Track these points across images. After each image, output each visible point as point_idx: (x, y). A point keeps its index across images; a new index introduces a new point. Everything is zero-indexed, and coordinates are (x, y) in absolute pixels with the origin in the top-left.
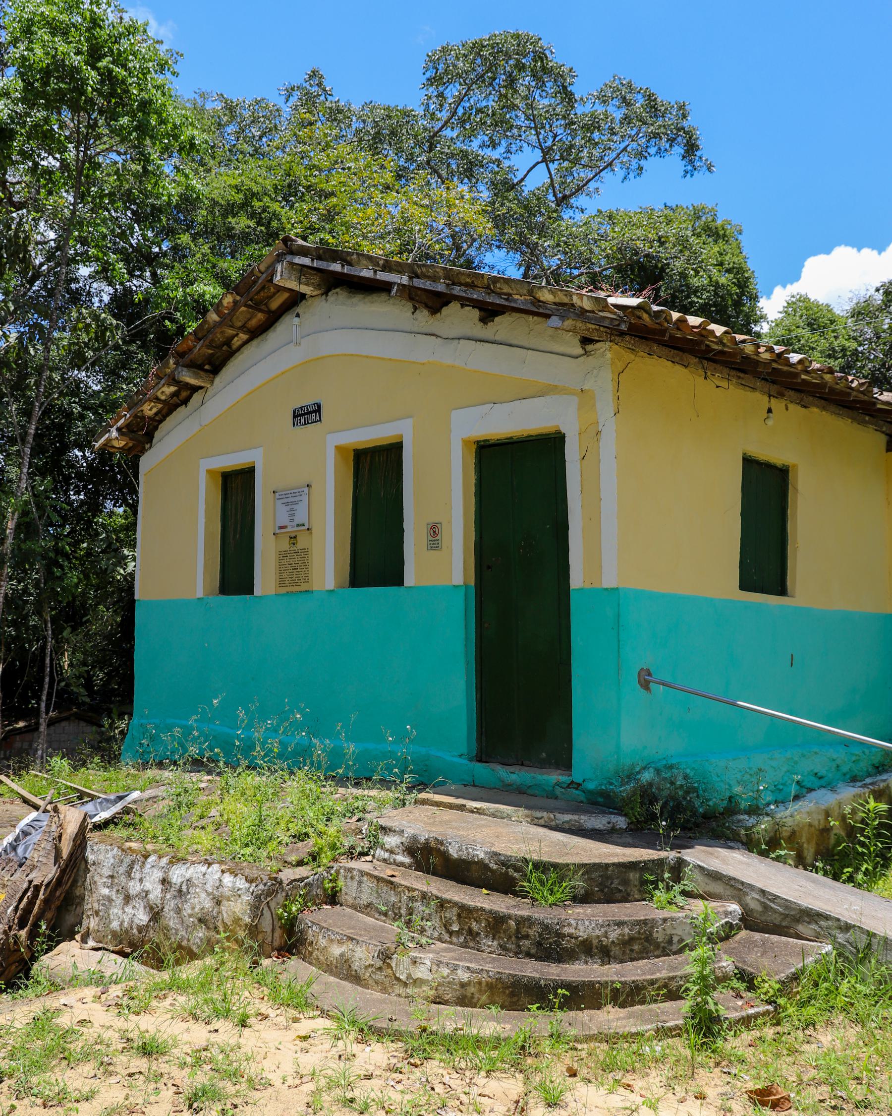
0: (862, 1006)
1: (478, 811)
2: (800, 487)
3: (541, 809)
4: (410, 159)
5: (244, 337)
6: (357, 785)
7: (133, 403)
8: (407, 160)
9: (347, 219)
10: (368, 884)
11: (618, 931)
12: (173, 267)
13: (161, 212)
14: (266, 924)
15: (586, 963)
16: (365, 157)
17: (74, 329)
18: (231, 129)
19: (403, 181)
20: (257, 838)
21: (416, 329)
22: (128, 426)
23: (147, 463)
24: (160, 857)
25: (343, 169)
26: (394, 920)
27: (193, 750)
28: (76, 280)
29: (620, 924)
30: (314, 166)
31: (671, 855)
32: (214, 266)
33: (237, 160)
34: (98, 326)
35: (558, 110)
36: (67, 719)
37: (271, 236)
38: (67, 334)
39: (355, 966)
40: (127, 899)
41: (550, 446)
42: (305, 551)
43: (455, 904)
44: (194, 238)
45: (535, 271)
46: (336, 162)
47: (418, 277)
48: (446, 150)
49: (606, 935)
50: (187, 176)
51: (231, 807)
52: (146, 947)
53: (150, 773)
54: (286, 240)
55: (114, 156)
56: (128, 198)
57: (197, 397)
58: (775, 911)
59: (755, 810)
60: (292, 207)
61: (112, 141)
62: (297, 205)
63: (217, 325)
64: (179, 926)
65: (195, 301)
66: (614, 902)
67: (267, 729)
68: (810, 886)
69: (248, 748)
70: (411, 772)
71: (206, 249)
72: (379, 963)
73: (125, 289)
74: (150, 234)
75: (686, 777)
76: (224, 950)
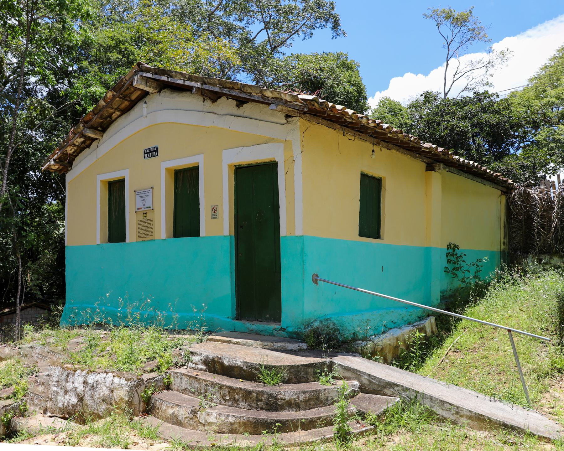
0: (413, 424)
1: (237, 343)
3: (267, 341)
4: (199, 26)
5: (118, 113)
6: (179, 333)
7: (61, 147)
8: (198, 26)
9: (168, 55)
10: (185, 379)
11: (304, 396)
12: (79, 78)
13: (73, 49)
14: (136, 400)
15: (289, 411)
16: (176, 24)
17: (28, 109)
18: (108, 7)
19: (196, 37)
20: (130, 360)
21: (205, 110)
22: (59, 158)
23: (69, 177)
24: (82, 371)
25: (166, 30)
26: (198, 395)
27: (97, 319)
28: (29, 84)
29: (304, 392)
30: (151, 28)
31: (328, 360)
32: (101, 78)
33: (111, 23)
34: (41, 108)
36: (30, 307)
37: (130, 63)
38: (25, 112)
39: (180, 418)
40: (66, 392)
41: (270, 168)
42: (151, 220)
43: (227, 387)
44: (90, 63)
45: (262, 83)
46: (162, 26)
47: (206, 84)
48: (217, 22)
49: (298, 398)
50: (85, 31)
51: (117, 346)
52: (77, 414)
53: (75, 331)
54: (139, 64)
55: (47, 19)
56: (55, 41)
57: (94, 144)
58: (375, 384)
59: (365, 339)
60: (140, 49)
61: (46, 12)
62: (142, 47)
63: (104, 107)
64: (92, 404)
65: (91, 95)
66: (302, 382)
67: (133, 307)
68: (390, 372)
69: (124, 317)
70: (204, 326)
71: (96, 69)
72: (191, 416)
73: (54, 89)
74: (67, 60)
75: (334, 324)
76: (115, 414)
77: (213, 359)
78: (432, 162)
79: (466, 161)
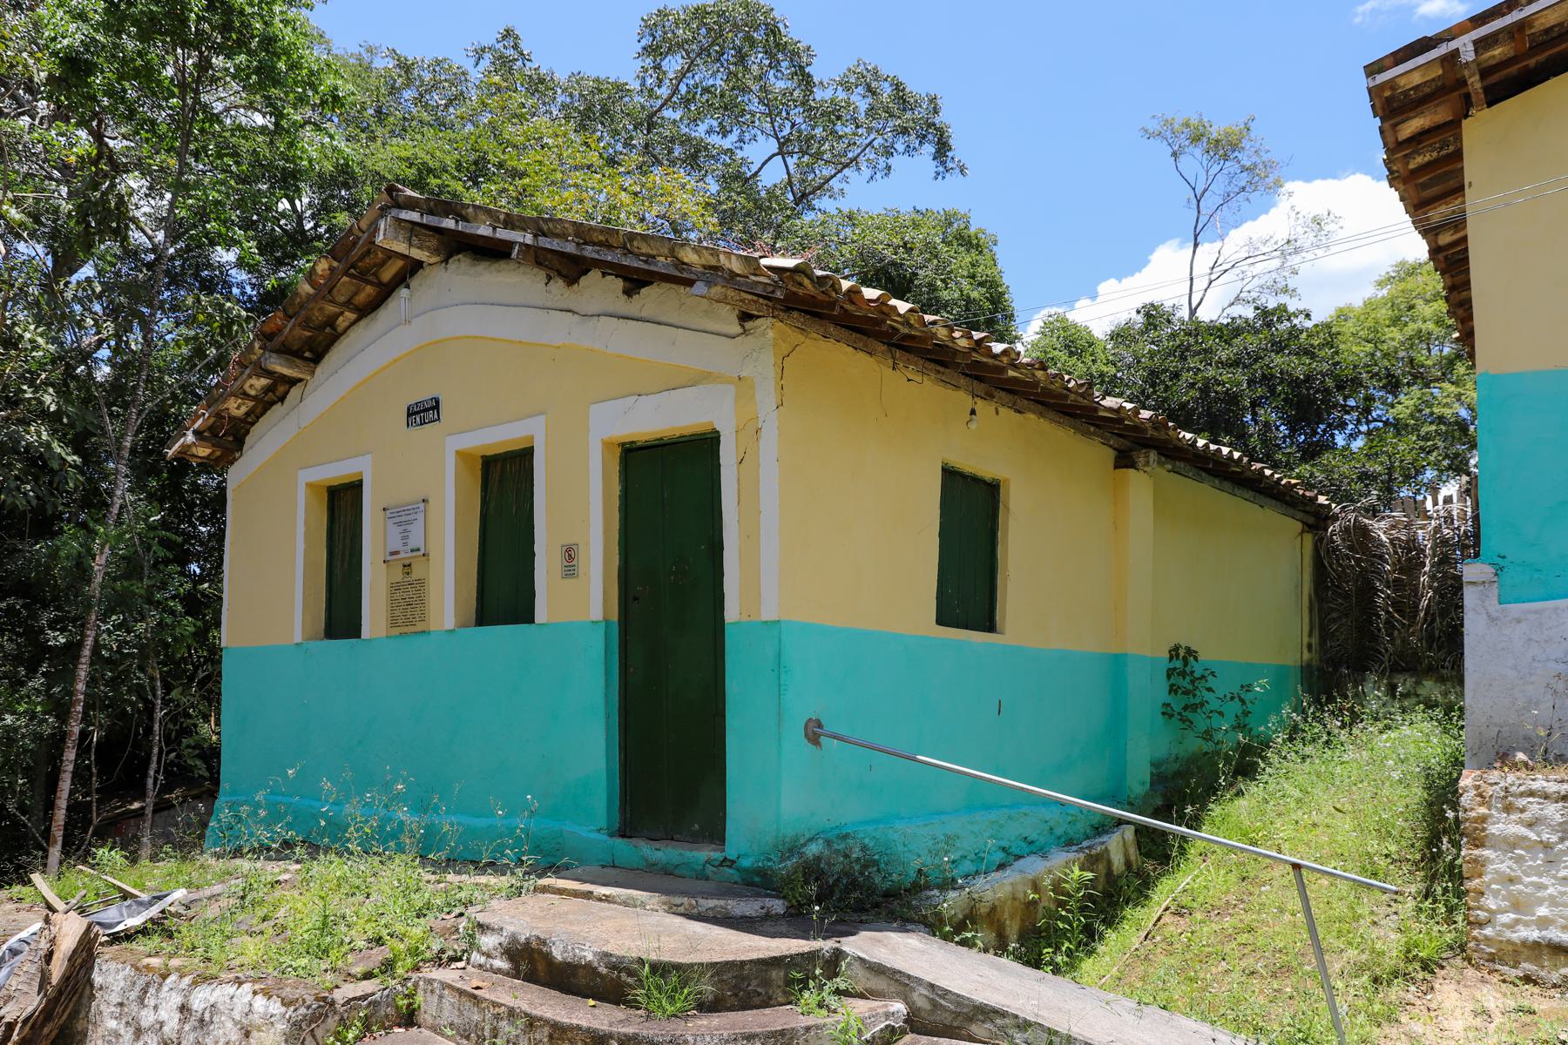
2: (1012, 506)
35: (796, 94)
77: (528, 942)
78: (1130, 445)
79: (1213, 447)
